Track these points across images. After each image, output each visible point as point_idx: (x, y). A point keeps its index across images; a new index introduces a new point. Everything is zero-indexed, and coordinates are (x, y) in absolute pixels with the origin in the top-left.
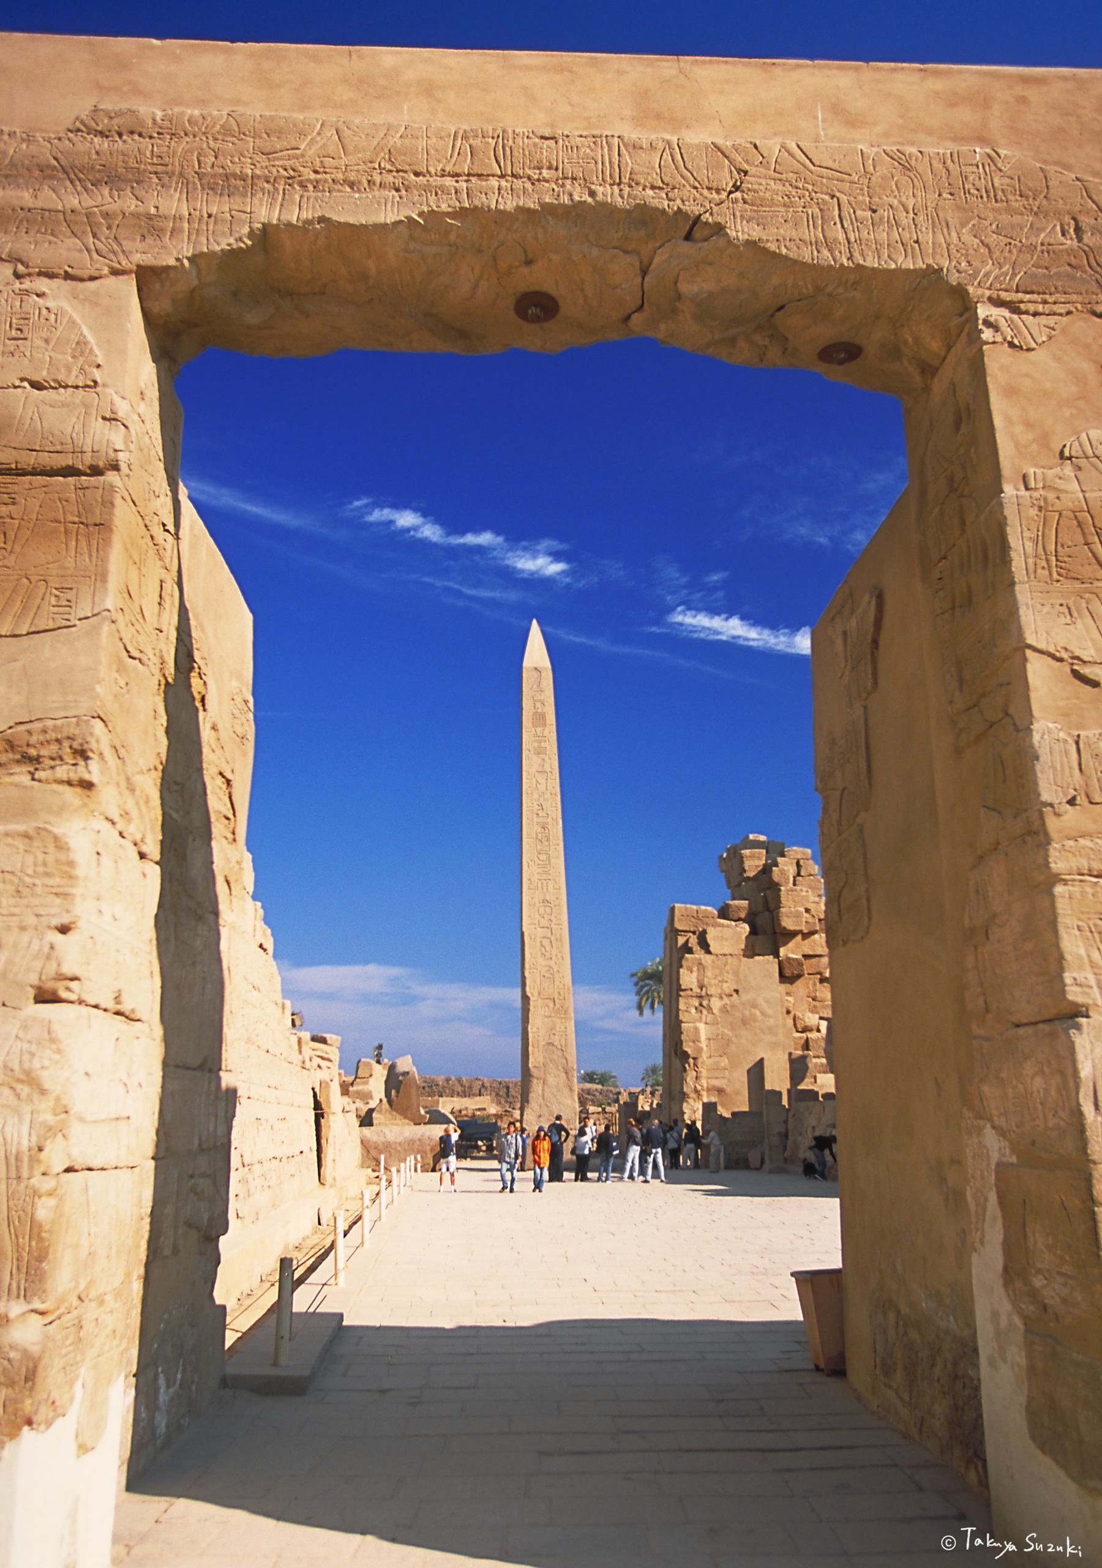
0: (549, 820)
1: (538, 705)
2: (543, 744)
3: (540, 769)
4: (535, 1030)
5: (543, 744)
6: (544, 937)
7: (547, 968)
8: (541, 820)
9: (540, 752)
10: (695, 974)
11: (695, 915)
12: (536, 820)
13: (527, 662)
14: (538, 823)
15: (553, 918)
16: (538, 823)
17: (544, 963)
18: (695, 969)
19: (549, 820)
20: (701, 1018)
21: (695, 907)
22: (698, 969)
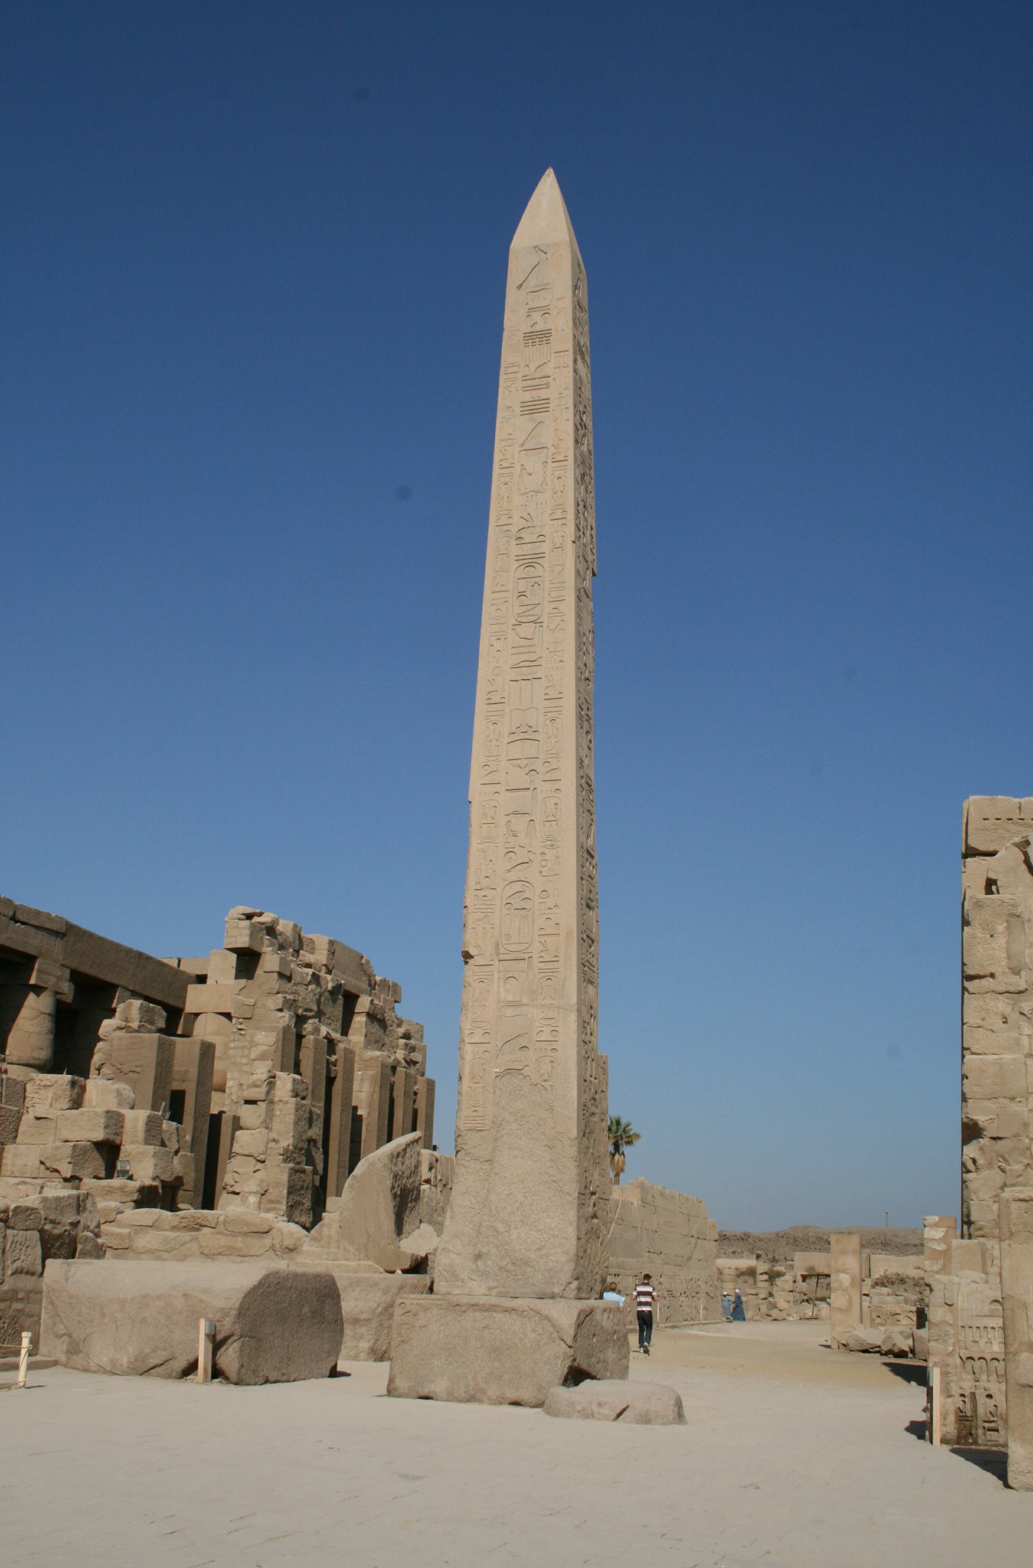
0: (545, 548)
1: (536, 316)
2: (543, 394)
3: (530, 445)
4: (477, 1038)
5: (543, 394)
6: (515, 813)
7: (518, 887)
8: (527, 549)
9: (534, 408)
10: (1001, 940)
11: (1016, 816)
12: (515, 550)
13: (522, 239)
14: (519, 558)
15: (538, 765)
16: (519, 558)
17: (513, 876)
18: (1001, 928)
19: (545, 548)
20: (1018, 1043)
21: (1017, 800)
22: (1008, 928)
